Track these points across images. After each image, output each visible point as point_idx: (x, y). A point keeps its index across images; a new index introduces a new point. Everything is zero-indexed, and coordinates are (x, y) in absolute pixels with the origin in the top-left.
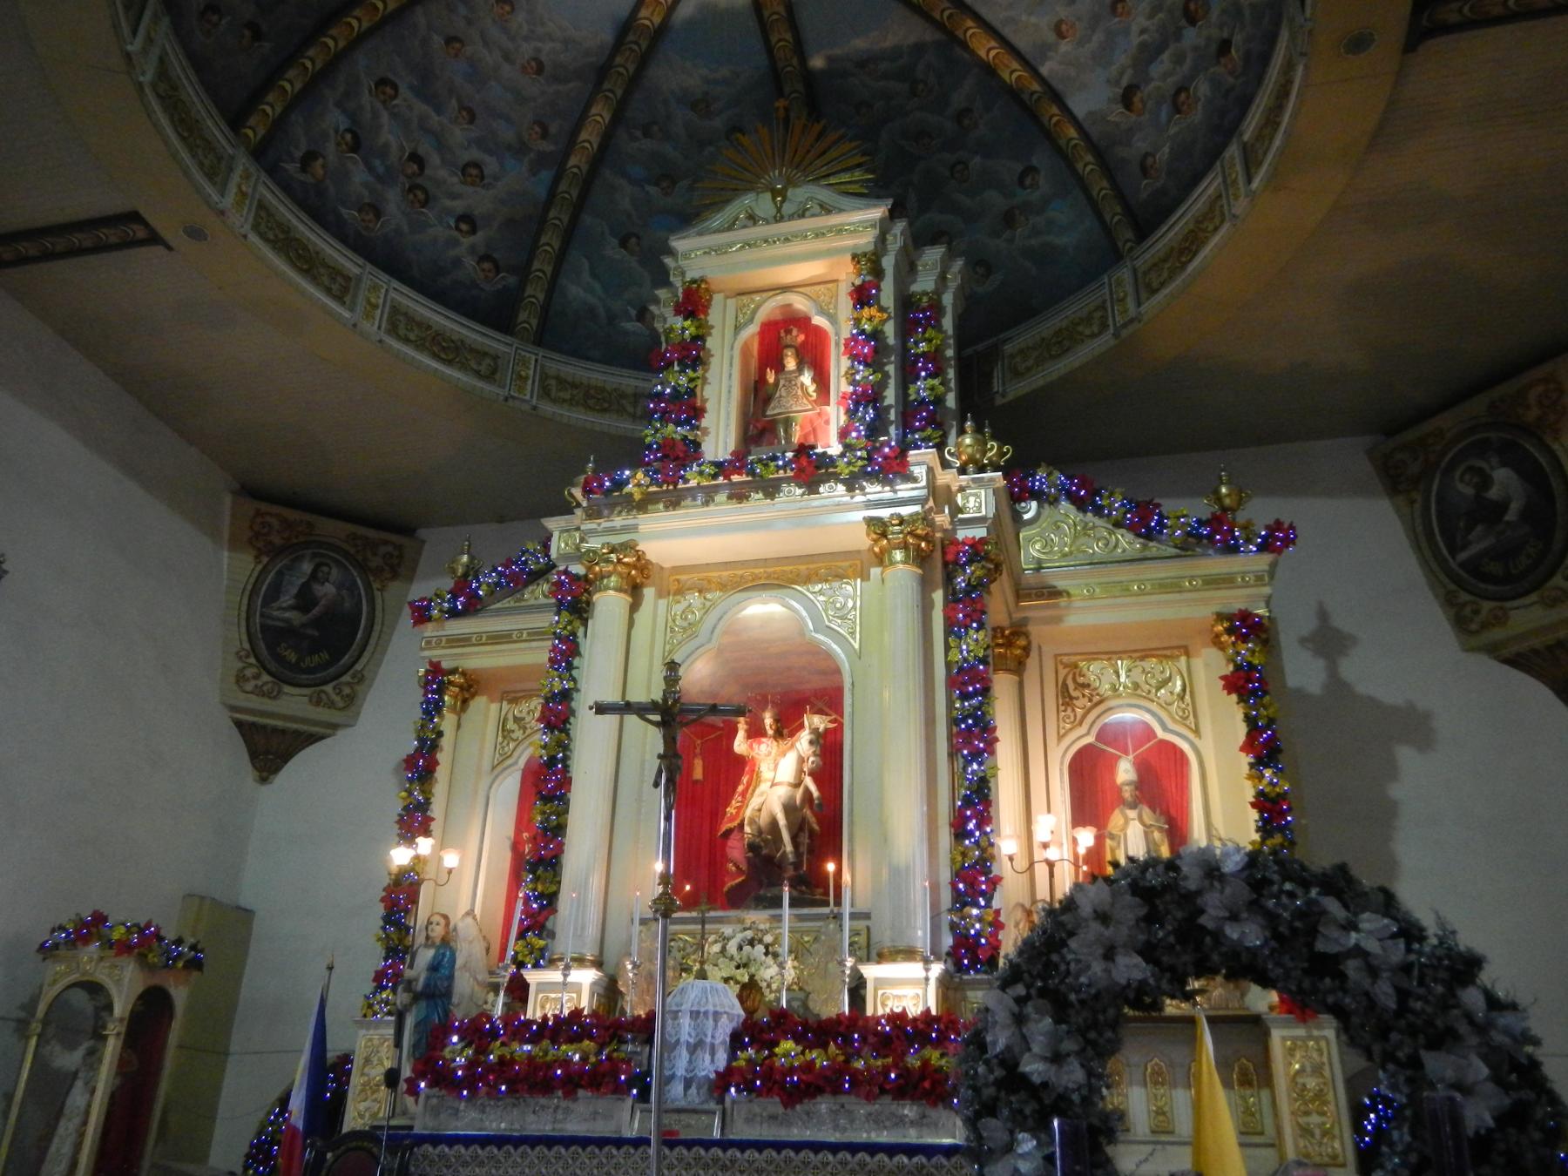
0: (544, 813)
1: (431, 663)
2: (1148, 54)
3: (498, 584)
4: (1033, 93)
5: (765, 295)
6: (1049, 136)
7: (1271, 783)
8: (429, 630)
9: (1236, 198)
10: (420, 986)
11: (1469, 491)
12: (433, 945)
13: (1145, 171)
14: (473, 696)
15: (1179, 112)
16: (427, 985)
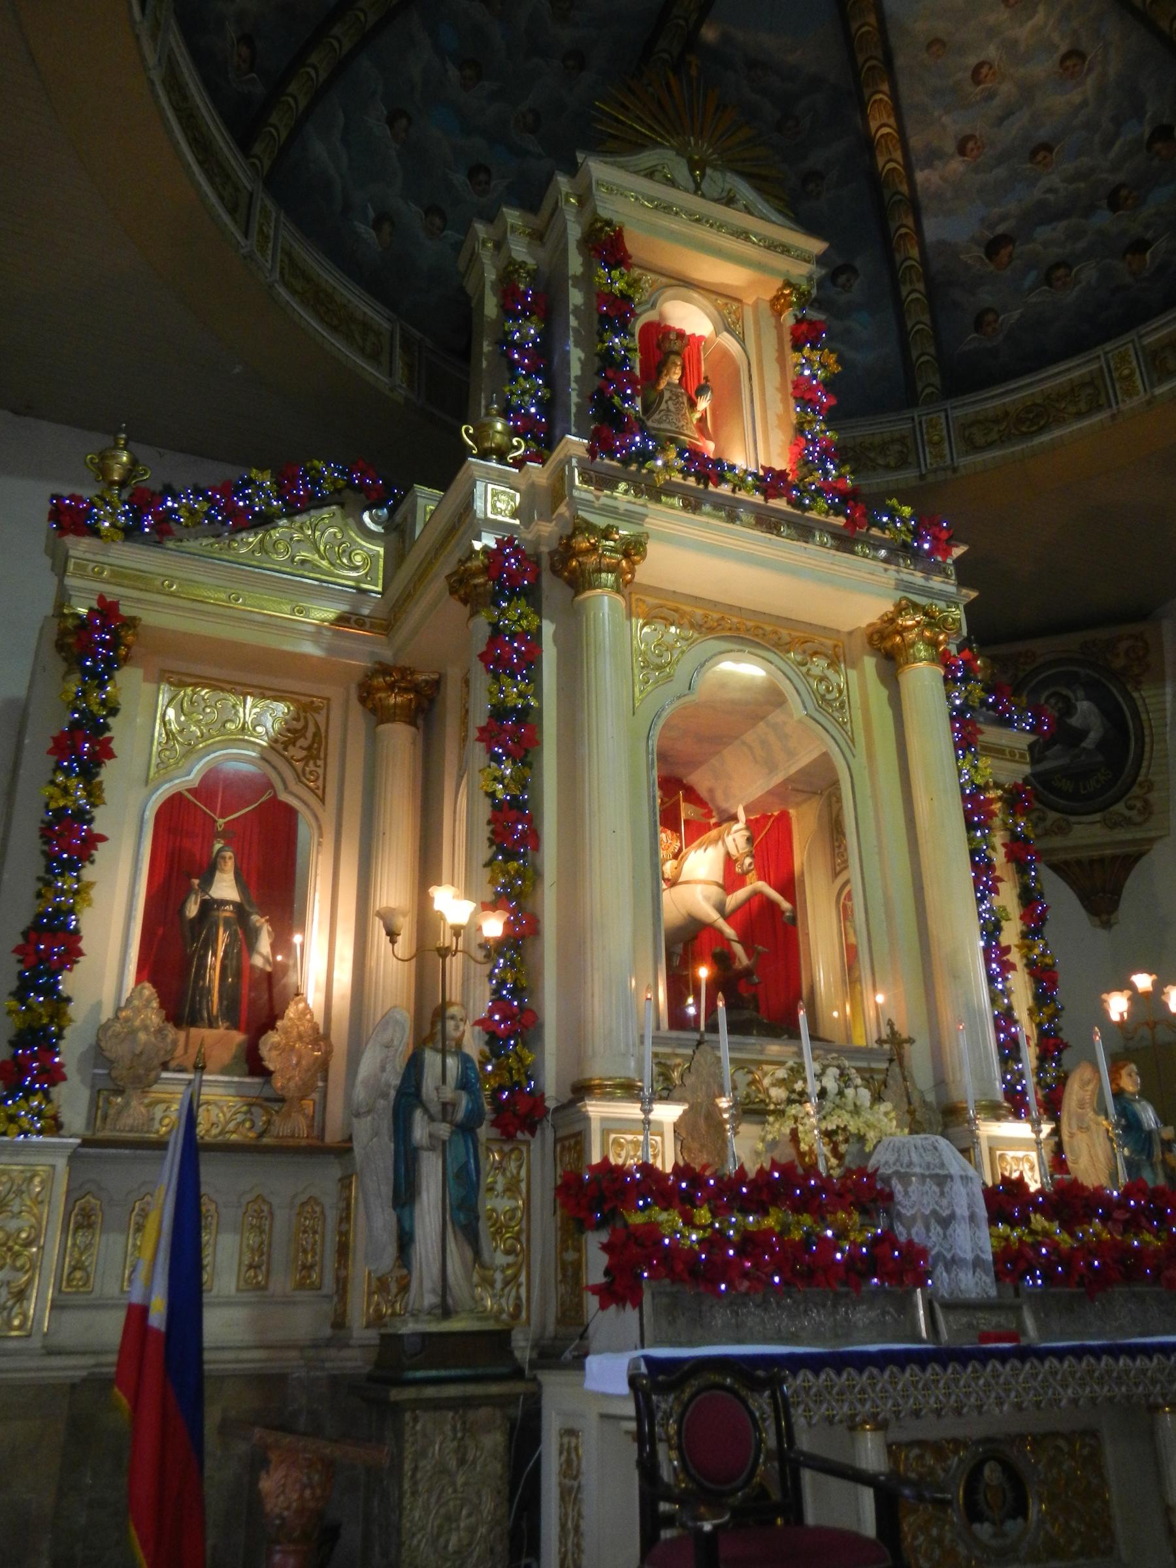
0: (506, 873)
1: (101, 599)
2: (1043, 214)
3: (207, 515)
4: (898, 193)
5: (664, 280)
6: (888, 247)
7: (1043, 954)
8: (80, 547)
9: (1130, 393)
10: (460, 1115)
15: (1051, 286)
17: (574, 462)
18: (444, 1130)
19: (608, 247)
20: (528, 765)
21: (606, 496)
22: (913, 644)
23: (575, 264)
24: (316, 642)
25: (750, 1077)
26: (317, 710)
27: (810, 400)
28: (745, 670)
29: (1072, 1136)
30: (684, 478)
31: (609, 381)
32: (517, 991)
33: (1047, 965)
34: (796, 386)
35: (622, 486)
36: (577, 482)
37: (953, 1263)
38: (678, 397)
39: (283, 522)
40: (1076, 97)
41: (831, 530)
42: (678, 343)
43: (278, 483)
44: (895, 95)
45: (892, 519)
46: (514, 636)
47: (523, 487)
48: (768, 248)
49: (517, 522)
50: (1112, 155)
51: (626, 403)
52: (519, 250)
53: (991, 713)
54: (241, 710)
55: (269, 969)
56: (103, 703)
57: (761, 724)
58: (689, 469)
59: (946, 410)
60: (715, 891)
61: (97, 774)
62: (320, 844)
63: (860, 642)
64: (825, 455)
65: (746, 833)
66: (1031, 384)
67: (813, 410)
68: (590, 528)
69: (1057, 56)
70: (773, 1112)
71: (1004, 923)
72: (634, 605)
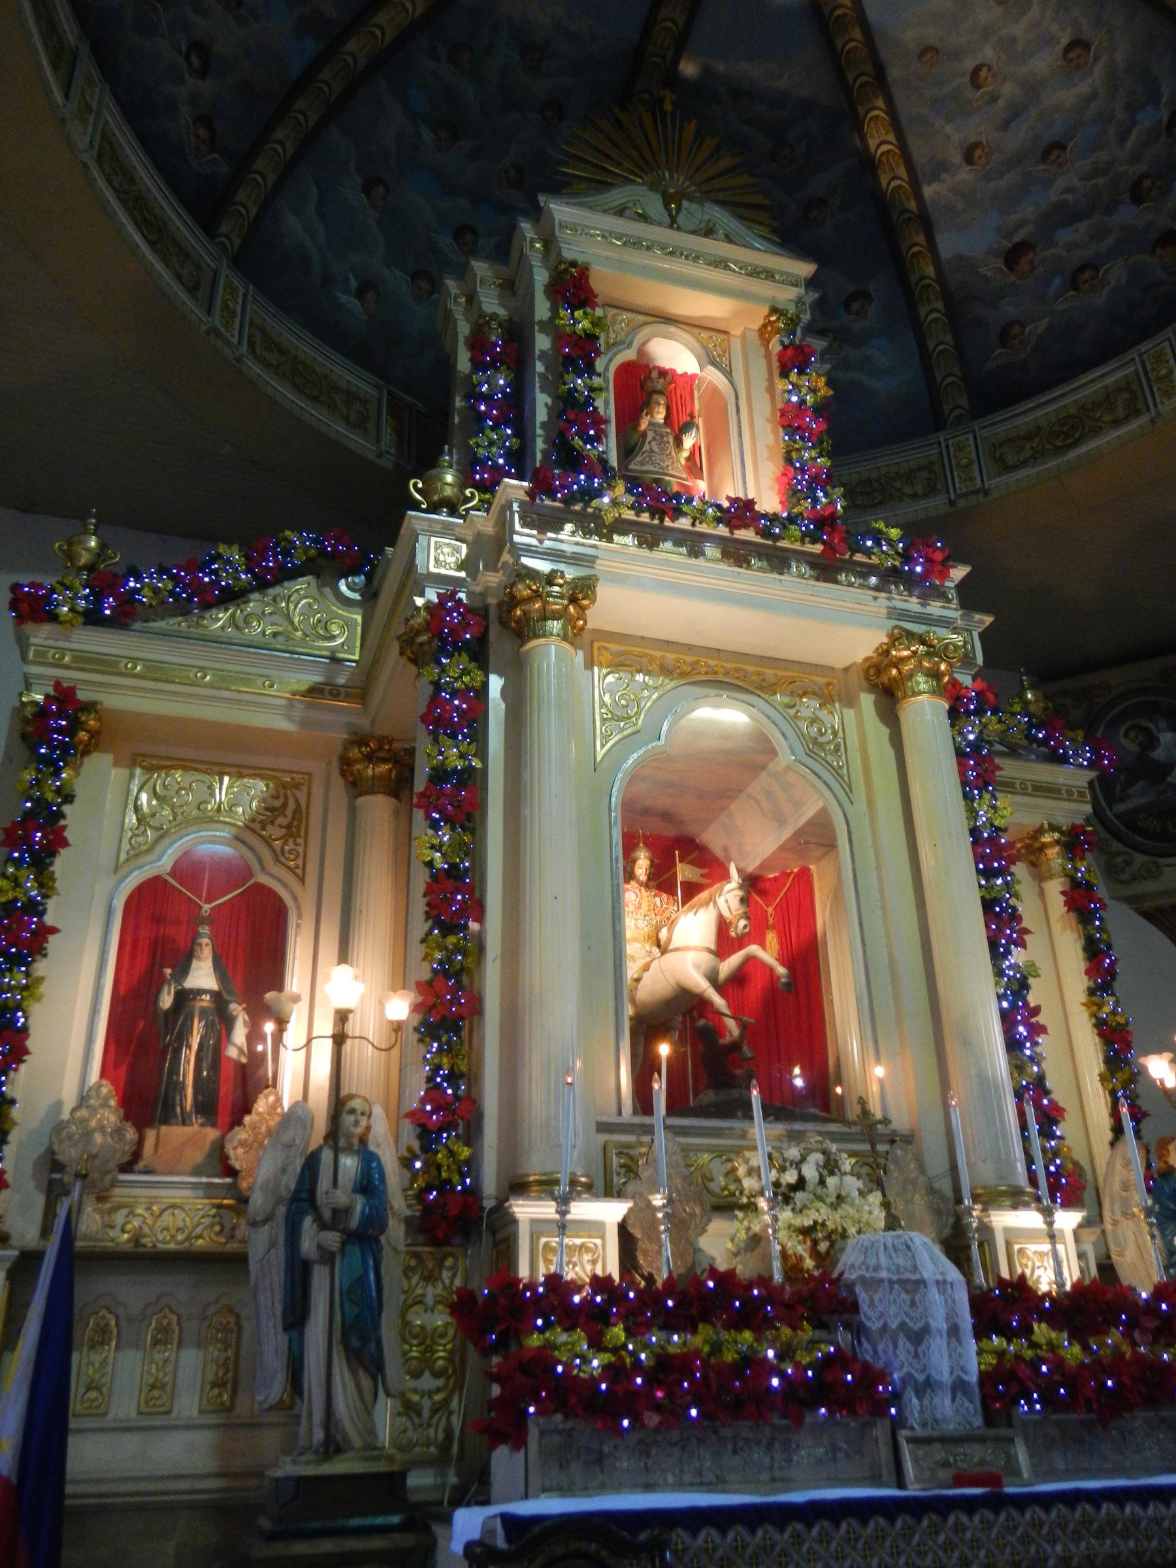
0: (442, 948)
1: (58, 685)
2: (1062, 215)
3: (172, 593)
5: (642, 318)
6: (900, 266)
7: (1114, 1012)
8: (41, 635)
10: (354, 1222)
11: (1134, 748)
12: (349, 1149)
13: (1004, 337)
14: (97, 748)
15: (1076, 289)
16: (366, 1220)
17: (515, 507)
18: (332, 1239)
19: (573, 287)
20: (473, 832)
21: (550, 539)
22: (911, 676)
23: (542, 309)
24: (289, 718)
25: (729, 1166)
26: (297, 786)
27: (799, 428)
28: (726, 717)
29: (1115, 1223)
30: (637, 515)
31: (571, 423)
32: (453, 1078)
33: (1119, 1024)
34: (783, 414)
35: (569, 527)
36: (517, 527)
37: (927, 1386)
38: (662, 437)
39: (255, 596)
40: (1084, 88)
41: (808, 558)
42: (662, 381)
43: (248, 558)
44: (891, 110)
45: (877, 543)
46: (455, 693)
47: (470, 538)
48: (750, 275)
49: (463, 574)
50: (1129, 145)
51: (593, 445)
52: (491, 303)
53: (1043, 749)
54: (217, 791)
55: (244, 1060)
56: (58, 791)
57: (763, 773)
58: (640, 504)
59: (974, 431)
60: (707, 959)
61: (51, 864)
62: (298, 926)
63: (856, 678)
64: (816, 482)
65: (740, 893)
66: (1063, 395)
67: (802, 438)
68: (533, 574)
69: (1060, 48)
70: (742, 1208)
71: (1031, 981)
72: (596, 654)
